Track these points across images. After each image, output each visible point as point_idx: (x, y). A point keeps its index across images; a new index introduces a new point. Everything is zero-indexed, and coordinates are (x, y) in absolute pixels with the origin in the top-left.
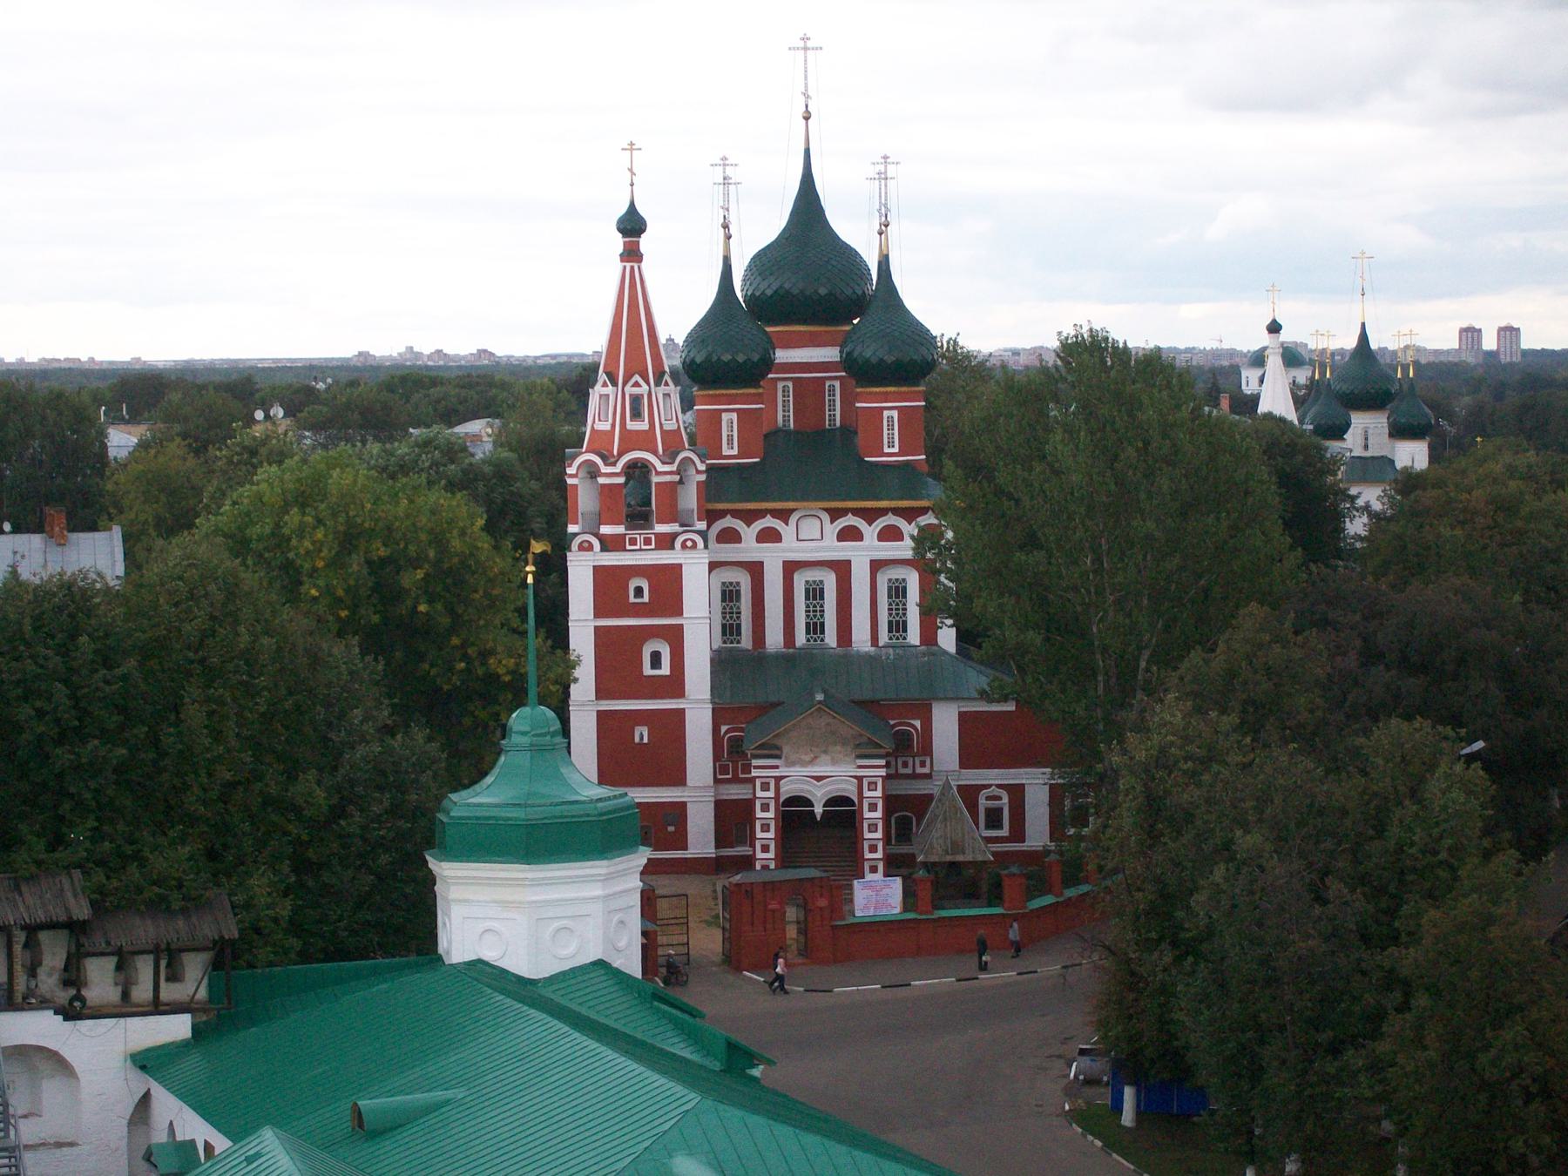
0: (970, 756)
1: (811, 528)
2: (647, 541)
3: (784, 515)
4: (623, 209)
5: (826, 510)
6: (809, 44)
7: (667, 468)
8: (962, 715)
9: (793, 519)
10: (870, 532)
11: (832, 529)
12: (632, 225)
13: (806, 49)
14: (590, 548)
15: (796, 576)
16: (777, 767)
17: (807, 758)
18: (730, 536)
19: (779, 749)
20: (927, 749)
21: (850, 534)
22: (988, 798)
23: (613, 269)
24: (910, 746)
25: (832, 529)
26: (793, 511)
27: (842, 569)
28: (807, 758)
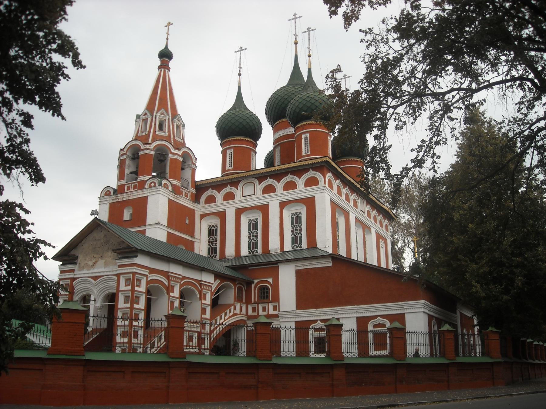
0: (304, 300)
1: (248, 190)
2: (135, 187)
3: (235, 183)
4: (163, 47)
5: (257, 178)
6: (297, 16)
7: (148, 147)
8: (299, 273)
9: (240, 186)
10: (279, 186)
11: (259, 188)
12: (165, 56)
13: (295, 18)
14: (109, 194)
15: (242, 217)
16: (73, 271)
17: (91, 263)
18: (211, 200)
19: (77, 258)
20: (276, 299)
21: (269, 189)
22: (316, 330)
23: (156, 72)
24: (268, 297)
25: (259, 188)
26: (240, 181)
27: (264, 209)
28: (91, 263)
